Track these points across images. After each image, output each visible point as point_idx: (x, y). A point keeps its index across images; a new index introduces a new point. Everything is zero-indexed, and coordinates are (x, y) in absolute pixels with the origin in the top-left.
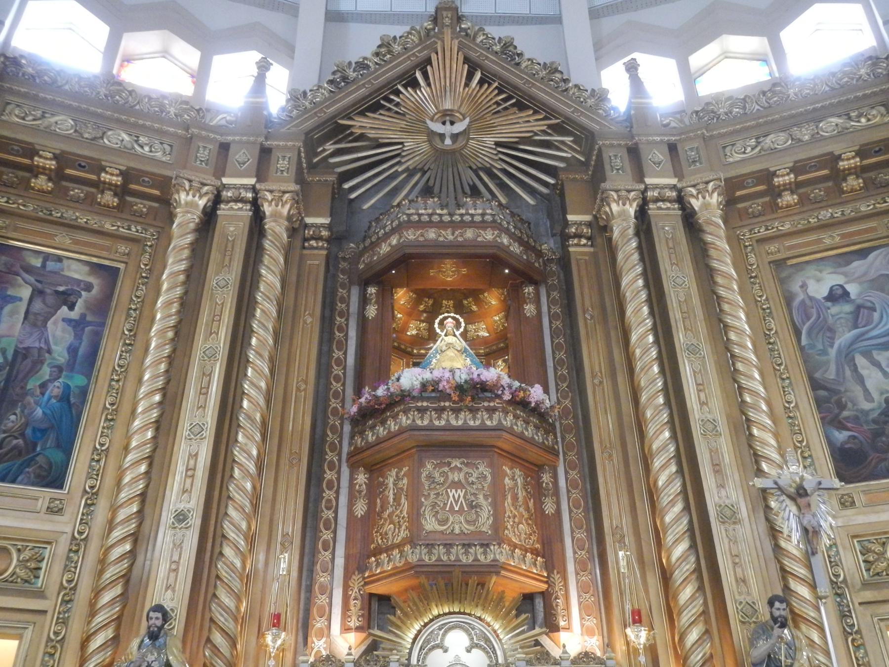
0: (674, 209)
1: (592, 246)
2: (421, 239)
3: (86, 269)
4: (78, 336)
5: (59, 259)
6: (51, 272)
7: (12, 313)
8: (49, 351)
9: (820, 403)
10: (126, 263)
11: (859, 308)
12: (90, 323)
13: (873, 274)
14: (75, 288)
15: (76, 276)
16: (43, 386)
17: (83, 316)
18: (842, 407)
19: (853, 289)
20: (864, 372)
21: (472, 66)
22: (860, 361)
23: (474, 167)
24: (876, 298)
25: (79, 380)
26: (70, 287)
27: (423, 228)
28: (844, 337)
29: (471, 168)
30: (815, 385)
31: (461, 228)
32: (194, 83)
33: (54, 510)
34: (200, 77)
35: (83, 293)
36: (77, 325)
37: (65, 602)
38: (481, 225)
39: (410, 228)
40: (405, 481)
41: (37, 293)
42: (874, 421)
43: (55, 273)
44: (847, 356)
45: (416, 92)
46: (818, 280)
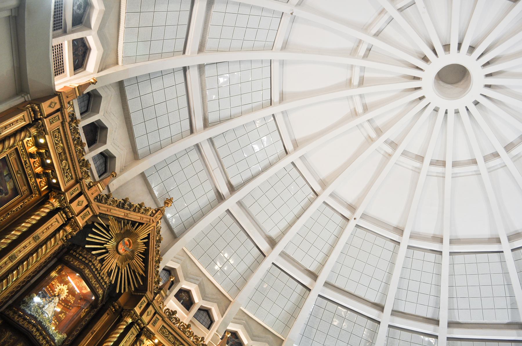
0: (138, 330)
1: (114, 313)
2: (87, 275)
3: (13, 187)
5: (11, 177)
6: (5, 179)
10: (22, 196)
14: (4, 191)
15: (8, 187)
23: (118, 265)
26: (3, 189)
27: (91, 272)
29: (117, 263)
31: (98, 282)
35: (4, 194)
38: (102, 286)
39: (89, 269)
40: (12, 341)
43: (6, 181)
45: (131, 227)
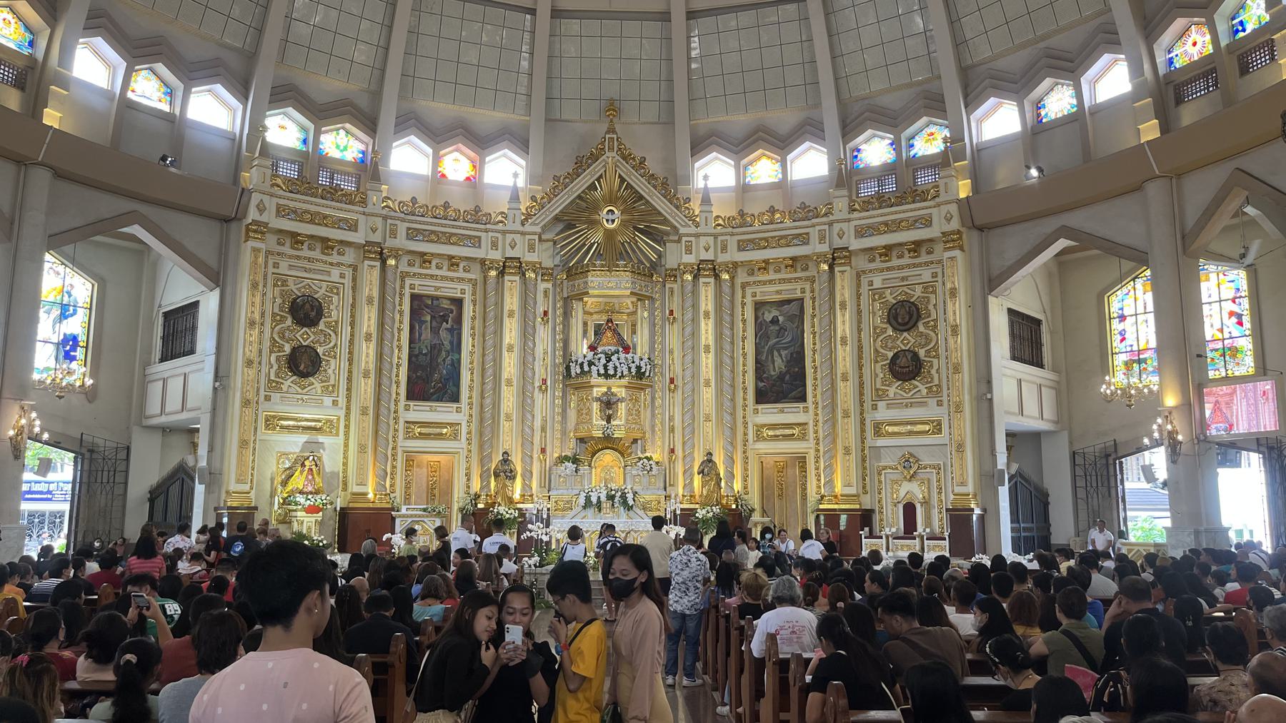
3: (449, 302)
4: (452, 336)
5: (437, 298)
7: (426, 328)
8: (443, 345)
9: (757, 370)
11: (781, 328)
12: (455, 329)
13: (791, 313)
16: (444, 360)
17: (452, 326)
18: (764, 373)
19: (781, 319)
20: (775, 359)
21: (622, 180)
22: (776, 353)
24: (788, 325)
25: (456, 356)
28: (770, 343)
30: (757, 361)
32: (474, 167)
33: (458, 410)
34: (478, 167)
36: (450, 330)
37: (469, 444)
41: (433, 317)
42: (774, 380)
44: (771, 351)
46: (770, 312)
